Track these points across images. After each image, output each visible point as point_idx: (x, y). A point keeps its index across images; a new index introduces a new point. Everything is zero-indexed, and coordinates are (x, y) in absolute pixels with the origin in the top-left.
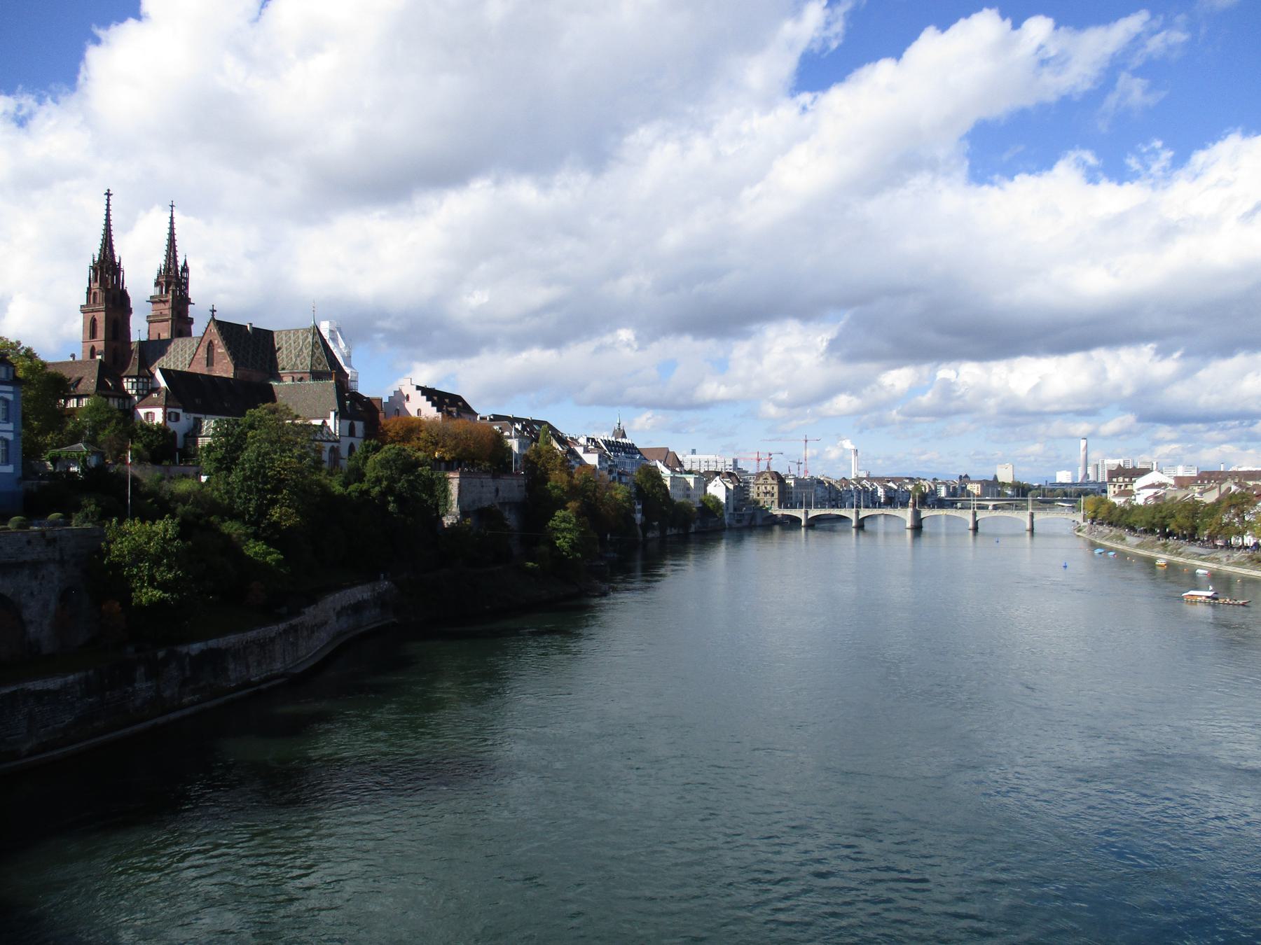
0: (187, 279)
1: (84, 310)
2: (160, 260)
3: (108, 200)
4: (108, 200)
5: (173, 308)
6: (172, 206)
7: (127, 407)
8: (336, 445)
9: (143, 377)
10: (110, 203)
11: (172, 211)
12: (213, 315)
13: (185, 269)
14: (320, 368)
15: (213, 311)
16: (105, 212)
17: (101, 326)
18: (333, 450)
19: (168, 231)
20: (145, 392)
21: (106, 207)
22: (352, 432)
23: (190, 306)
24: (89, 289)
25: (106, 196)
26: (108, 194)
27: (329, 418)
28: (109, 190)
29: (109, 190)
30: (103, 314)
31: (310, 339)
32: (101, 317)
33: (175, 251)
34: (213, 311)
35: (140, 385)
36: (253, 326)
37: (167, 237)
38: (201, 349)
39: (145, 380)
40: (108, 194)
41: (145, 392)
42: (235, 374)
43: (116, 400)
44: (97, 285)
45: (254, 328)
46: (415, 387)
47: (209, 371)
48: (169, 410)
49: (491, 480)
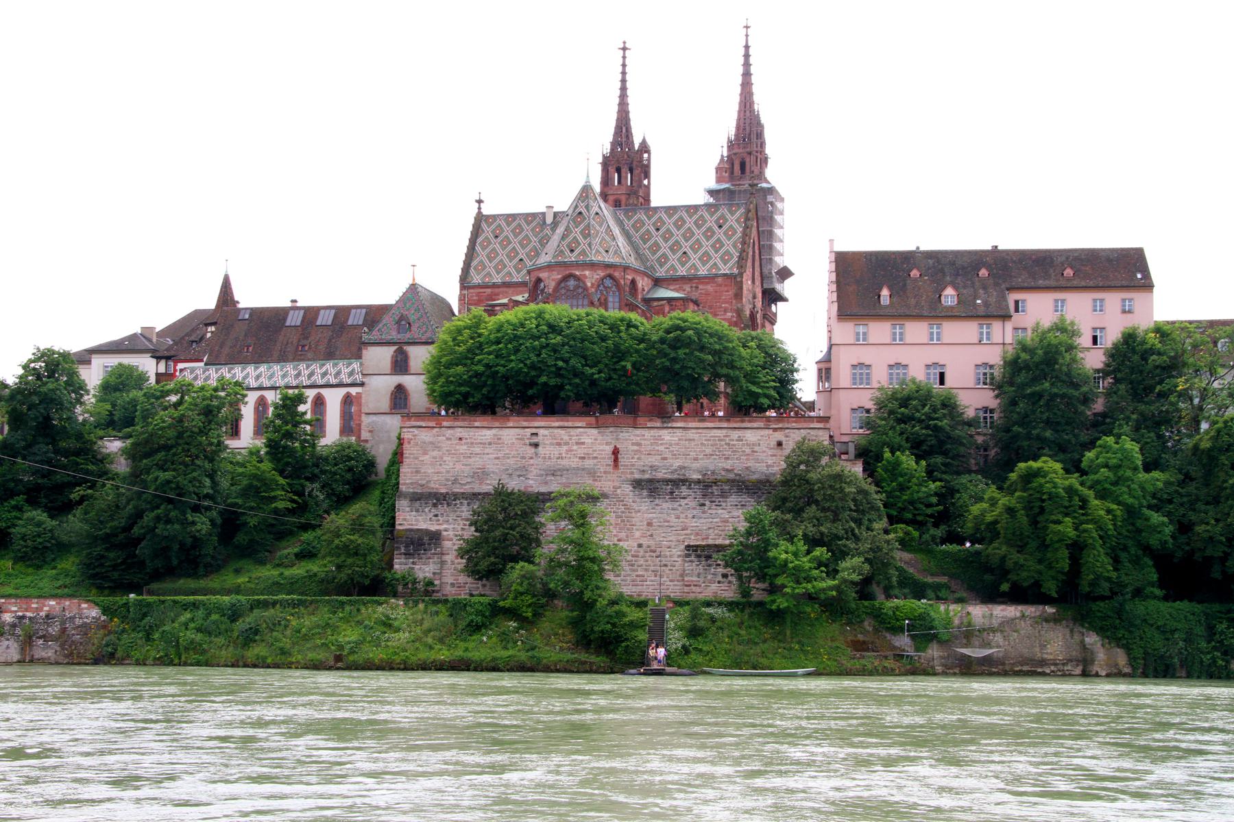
3: (624, 57)
4: (624, 57)
6: (747, 27)
8: (354, 391)
11: (747, 36)
12: (479, 208)
15: (480, 202)
18: (347, 401)
22: (400, 365)
25: (622, 52)
26: (624, 49)
28: (624, 43)
29: (624, 43)
34: (480, 202)
36: (555, 210)
40: (624, 49)
45: (556, 214)
48: (180, 366)
49: (595, 431)
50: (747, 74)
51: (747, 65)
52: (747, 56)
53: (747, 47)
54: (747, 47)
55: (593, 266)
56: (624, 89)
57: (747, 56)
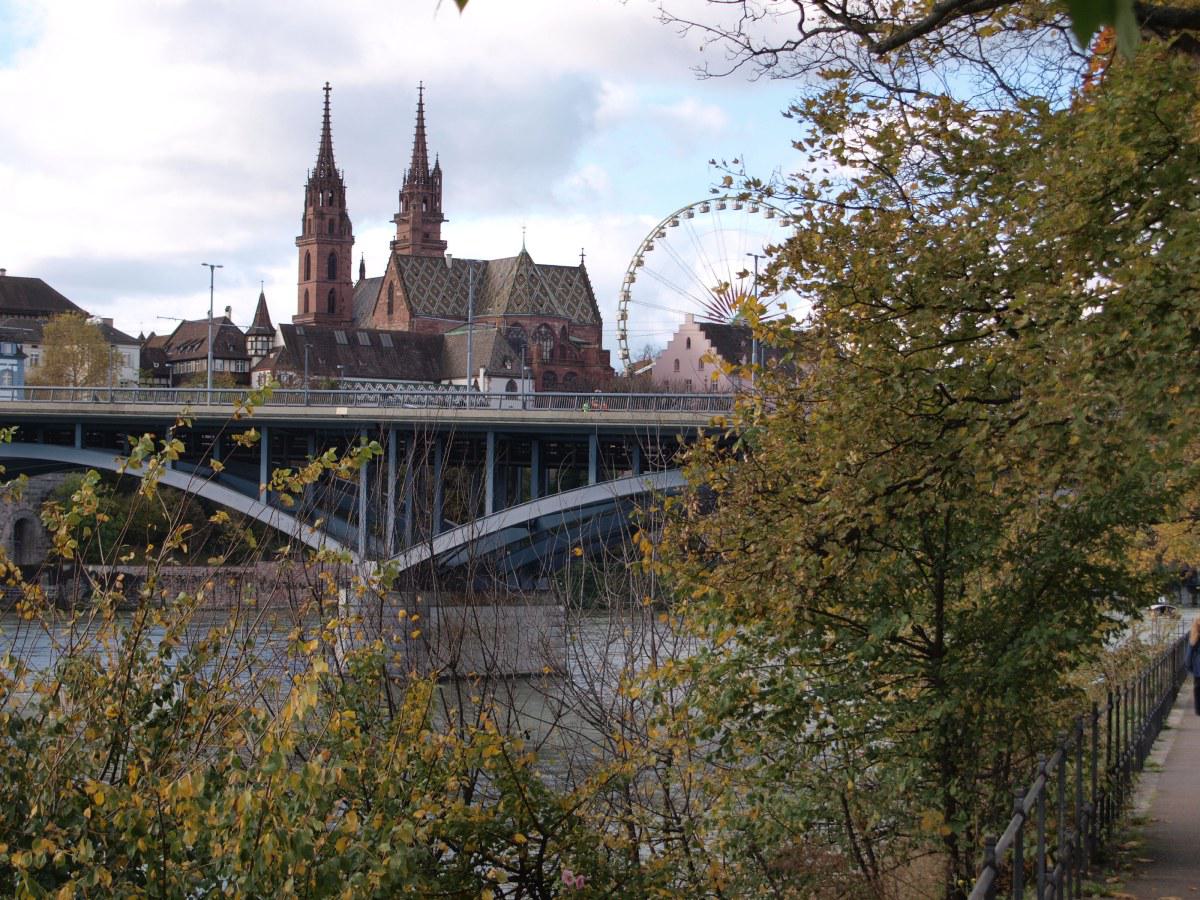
0: (440, 186)
1: (301, 242)
2: (406, 162)
3: (327, 96)
4: (327, 96)
5: (414, 230)
7: (247, 370)
9: (263, 335)
10: (330, 100)
13: (438, 172)
14: (518, 310)
16: (323, 113)
17: (314, 262)
19: (416, 123)
20: (264, 353)
21: (324, 106)
23: (443, 225)
24: (305, 216)
27: (478, 376)
30: (315, 246)
31: (514, 272)
32: (314, 249)
33: (424, 150)
35: (259, 346)
37: (414, 131)
38: (383, 293)
39: (265, 339)
40: (327, 89)
41: (264, 353)
42: (411, 324)
43: (233, 363)
44: (311, 209)
46: (697, 327)
47: (390, 320)
50: (421, 127)
51: (421, 119)
52: (421, 111)
53: (421, 104)
54: (421, 104)
55: (558, 318)
56: (327, 123)
57: (421, 111)
